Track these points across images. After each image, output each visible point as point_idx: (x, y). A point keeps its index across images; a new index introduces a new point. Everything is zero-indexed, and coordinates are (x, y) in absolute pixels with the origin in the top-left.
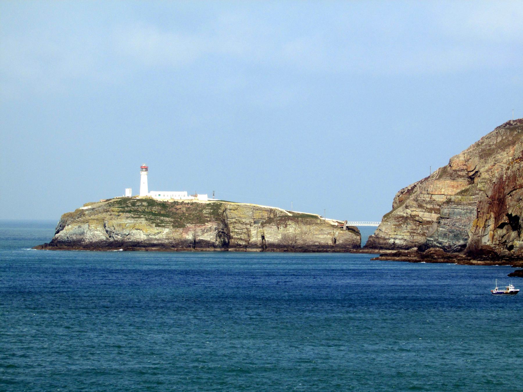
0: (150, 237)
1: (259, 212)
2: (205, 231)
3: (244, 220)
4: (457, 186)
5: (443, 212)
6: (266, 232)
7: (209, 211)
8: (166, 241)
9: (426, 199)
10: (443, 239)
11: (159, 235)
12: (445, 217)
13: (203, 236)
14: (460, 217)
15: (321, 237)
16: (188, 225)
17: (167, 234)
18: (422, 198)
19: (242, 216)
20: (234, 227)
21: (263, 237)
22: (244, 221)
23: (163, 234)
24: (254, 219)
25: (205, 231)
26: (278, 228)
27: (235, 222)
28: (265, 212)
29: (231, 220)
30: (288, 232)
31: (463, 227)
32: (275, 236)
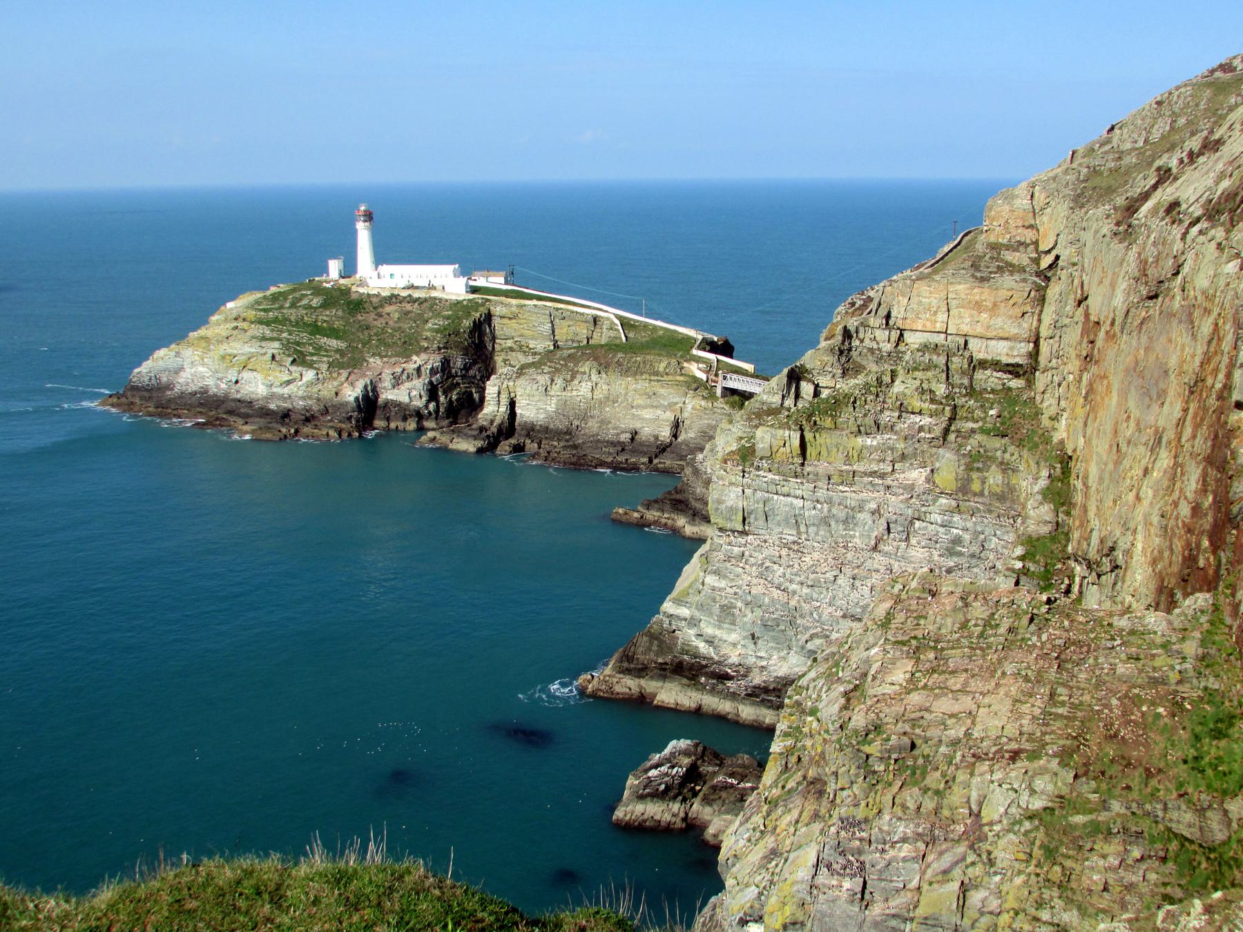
0: (275, 390)
1: (568, 323)
2: (404, 377)
4: (995, 305)
5: (720, 502)
6: (519, 391)
7: (441, 323)
8: (301, 403)
9: (881, 345)
10: (720, 628)
11: (291, 386)
12: (729, 526)
13: (396, 391)
14: (799, 533)
15: (647, 414)
16: (371, 360)
17: (310, 384)
18: (867, 343)
19: (526, 332)
20: (505, 361)
21: (512, 404)
22: (531, 346)
23: (300, 383)
25: (404, 377)
26: (552, 381)
27: (511, 349)
29: (503, 342)
30: (575, 393)
31: (806, 590)
32: (541, 405)
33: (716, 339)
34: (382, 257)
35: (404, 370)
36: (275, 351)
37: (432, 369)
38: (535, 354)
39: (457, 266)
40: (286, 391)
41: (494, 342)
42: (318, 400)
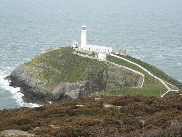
0: (37, 85)
1: (130, 76)
2: (73, 88)
3: (118, 81)
11: (42, 85)
17: (46, 85)
22: (118, 82)
24: (126, 82)
28: (135, 77)
33: (177, 91)
34: (89, 42)
35: (73, 85)
36: (41, 72)
37: (81, 86)
38: (119, 85)
40: (40, 86)
41: (107, 79)
42: (46, 91)
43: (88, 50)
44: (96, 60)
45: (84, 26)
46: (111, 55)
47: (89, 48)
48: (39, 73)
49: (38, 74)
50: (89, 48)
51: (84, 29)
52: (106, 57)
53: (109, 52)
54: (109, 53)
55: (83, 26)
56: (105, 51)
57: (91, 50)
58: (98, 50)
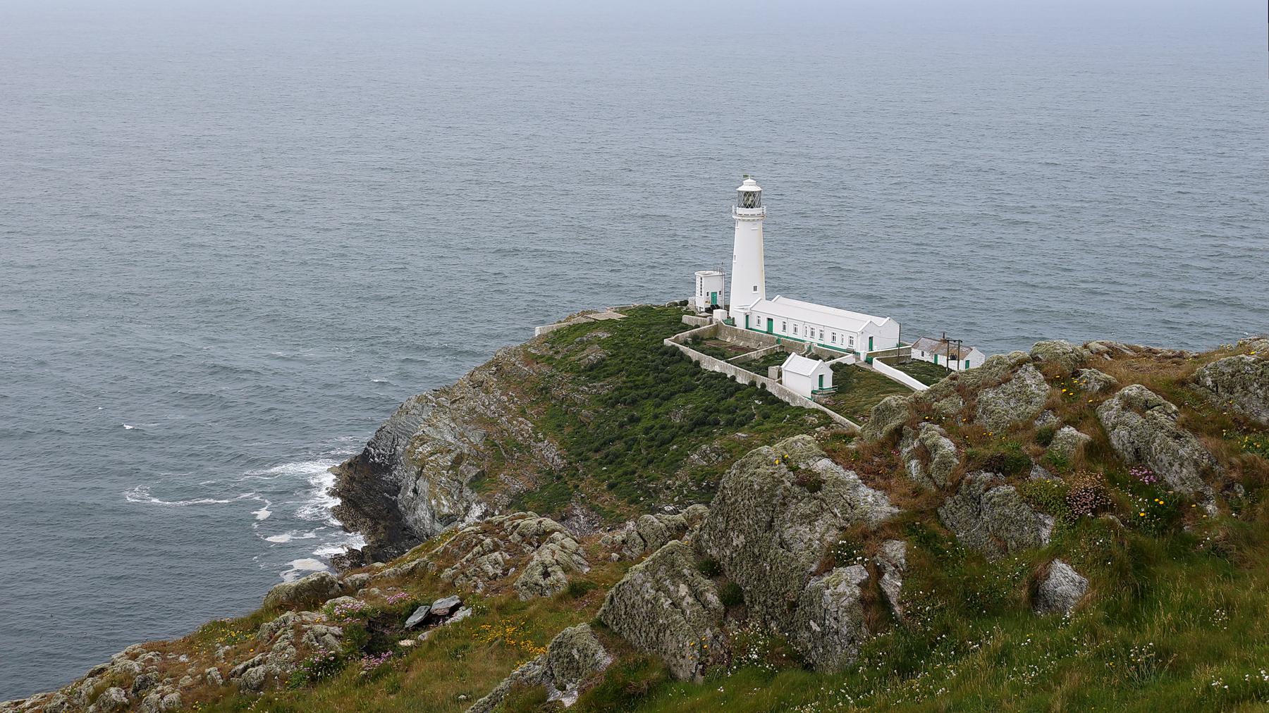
39: (881, 321)
43: (764, 327)
44: (764, 393)
45: (749, 186)
46: (879, 367)
47: (770, 320)
48: (454, 455)
49: (447, 460)
50: (770, 320)
51: (750, 200)
52: (828, 384)
53: (875, 349)
54: (869, 361)
55: (744, 188)
56: (851, 342)
57: (777, 329)
58: (812, 333)
